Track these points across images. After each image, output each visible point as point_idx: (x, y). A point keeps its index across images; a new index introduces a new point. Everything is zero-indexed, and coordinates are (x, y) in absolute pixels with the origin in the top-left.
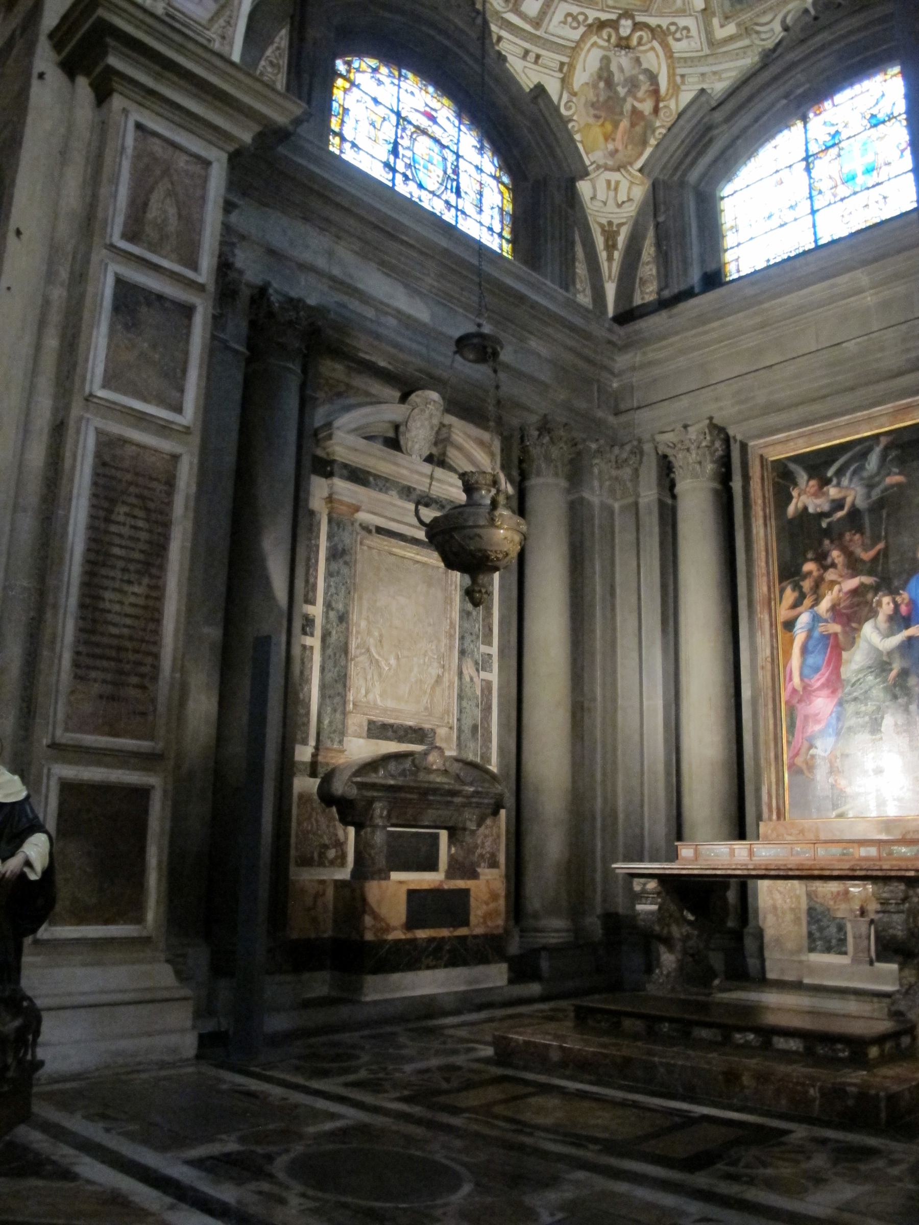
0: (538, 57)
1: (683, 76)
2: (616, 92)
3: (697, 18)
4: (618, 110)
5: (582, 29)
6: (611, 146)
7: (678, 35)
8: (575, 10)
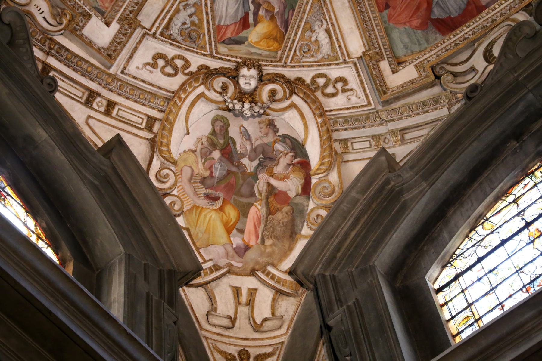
0: (111, 105)
1: (345, 141)
2: (240, 165)
3: (355, 65)
4: (245, 190)
5: (180, 78)
6: (237, 240)
7: (330, 90)
8: (171, 51)
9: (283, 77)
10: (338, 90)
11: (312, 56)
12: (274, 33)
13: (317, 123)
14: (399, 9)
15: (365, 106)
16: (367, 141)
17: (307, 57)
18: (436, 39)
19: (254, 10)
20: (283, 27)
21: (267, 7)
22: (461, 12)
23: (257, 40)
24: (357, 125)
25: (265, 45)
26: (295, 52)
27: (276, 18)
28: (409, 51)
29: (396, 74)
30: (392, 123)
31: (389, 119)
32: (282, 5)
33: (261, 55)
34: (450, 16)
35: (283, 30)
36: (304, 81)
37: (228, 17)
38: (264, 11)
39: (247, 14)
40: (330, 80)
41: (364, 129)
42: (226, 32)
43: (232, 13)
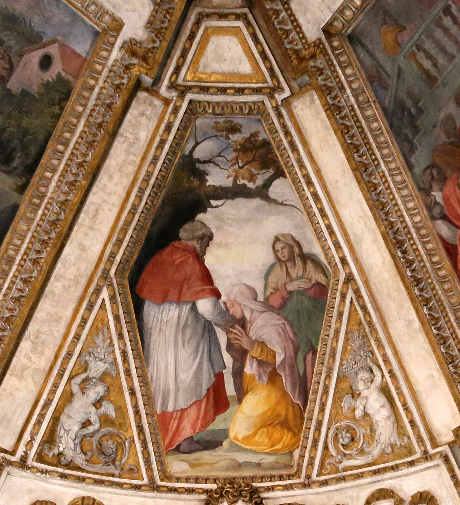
19: (234, 366)
20: (297, 394)
21: (261, 354)
25: (266, 441)
27: (281, 376)
33: (258, 465)
37: (181, 390)
39: (220, 377)
42: (182, 426)
43: (188, 381)
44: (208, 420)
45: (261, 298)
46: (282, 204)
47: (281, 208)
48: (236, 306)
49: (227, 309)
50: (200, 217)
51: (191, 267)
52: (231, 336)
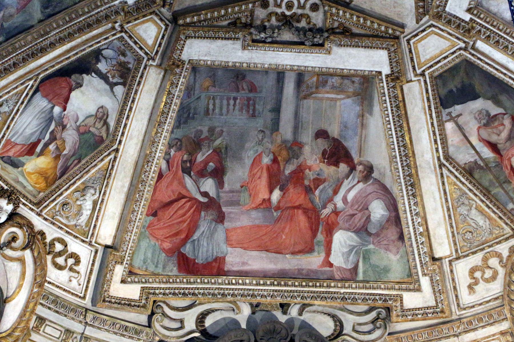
1: (41, 320)
3: (96, 252)
7: (60, 261)
9: (30, 225)
10: (67, 266)
11: (67, 218)
12: (50, 172)
13: (32, 291)
14: (162, 224)
15: (80, 297)
16: (60, 330)
17: (62, 216)
18: (171, 271)
22: (205, 263)
23: (31, 171)
24: (62, 310)
26: (56, 204)
28: (145, 267)
29: (123, 285)
30: (91, 328)
31: (91, 323)
32: (73, 151)
34: (195, 259)
35: (58, 175)
36: (45, 238)
38: (55, 147)
40: (67, 251)
41: (65, 318)
43: (27, 134)
44: (21, 155)
45: (78, 124)
46: (115, 96)
47: (113, 97)
48: (67, 119)
49: (63, 118)
50: (84, 75)
51: (65, 91)
52: (56, 129)
